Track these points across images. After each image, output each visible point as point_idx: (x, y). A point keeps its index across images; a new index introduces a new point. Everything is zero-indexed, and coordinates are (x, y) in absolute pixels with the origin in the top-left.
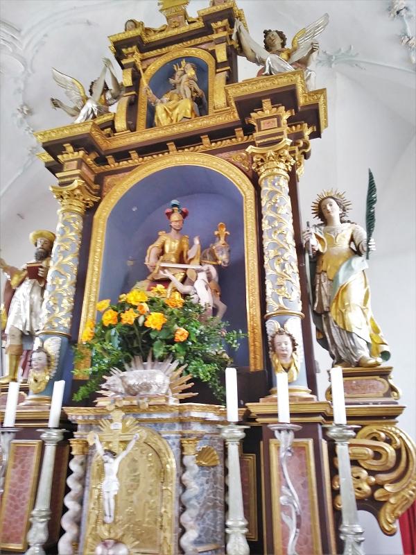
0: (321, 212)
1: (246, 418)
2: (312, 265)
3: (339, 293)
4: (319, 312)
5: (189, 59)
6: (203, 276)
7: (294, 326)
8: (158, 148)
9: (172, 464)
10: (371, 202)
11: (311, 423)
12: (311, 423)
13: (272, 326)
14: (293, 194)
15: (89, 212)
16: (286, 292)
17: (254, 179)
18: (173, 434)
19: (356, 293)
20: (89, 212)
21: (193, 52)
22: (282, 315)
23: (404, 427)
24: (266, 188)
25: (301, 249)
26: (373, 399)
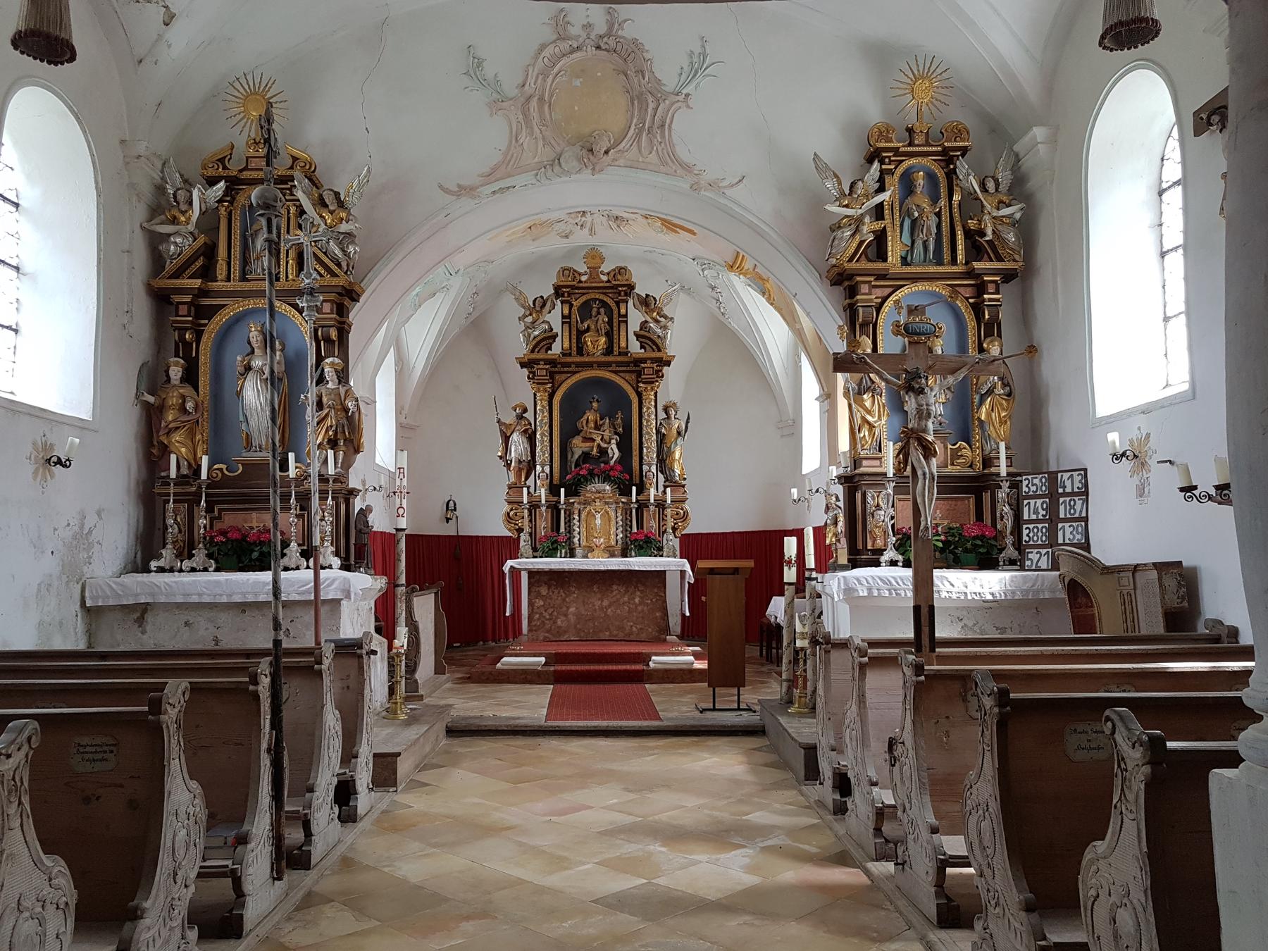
0: (666, 409)
1: (637, 501)
2: (661, 439)
3: (671, 452)
4: (663, 462)
5: (601, 301)
6: (613, 441)
7: (654, 469)
8: (589, 365)
9: (613, 515)
10: (687, 422)
11: (661, 505)
12: (661, 505)
13: (645, 468)
14: (656, 407)
15: (551, 396)
16: (651, 454)
17: (639, 395)
18: (613, 506)
19: (677, 455)
20: (551, 396)
21: (602, 297)
22: (650, 465)
23: (686, 506)
24: (645, 404)
25: (658, 431)
26: (679, 496)
